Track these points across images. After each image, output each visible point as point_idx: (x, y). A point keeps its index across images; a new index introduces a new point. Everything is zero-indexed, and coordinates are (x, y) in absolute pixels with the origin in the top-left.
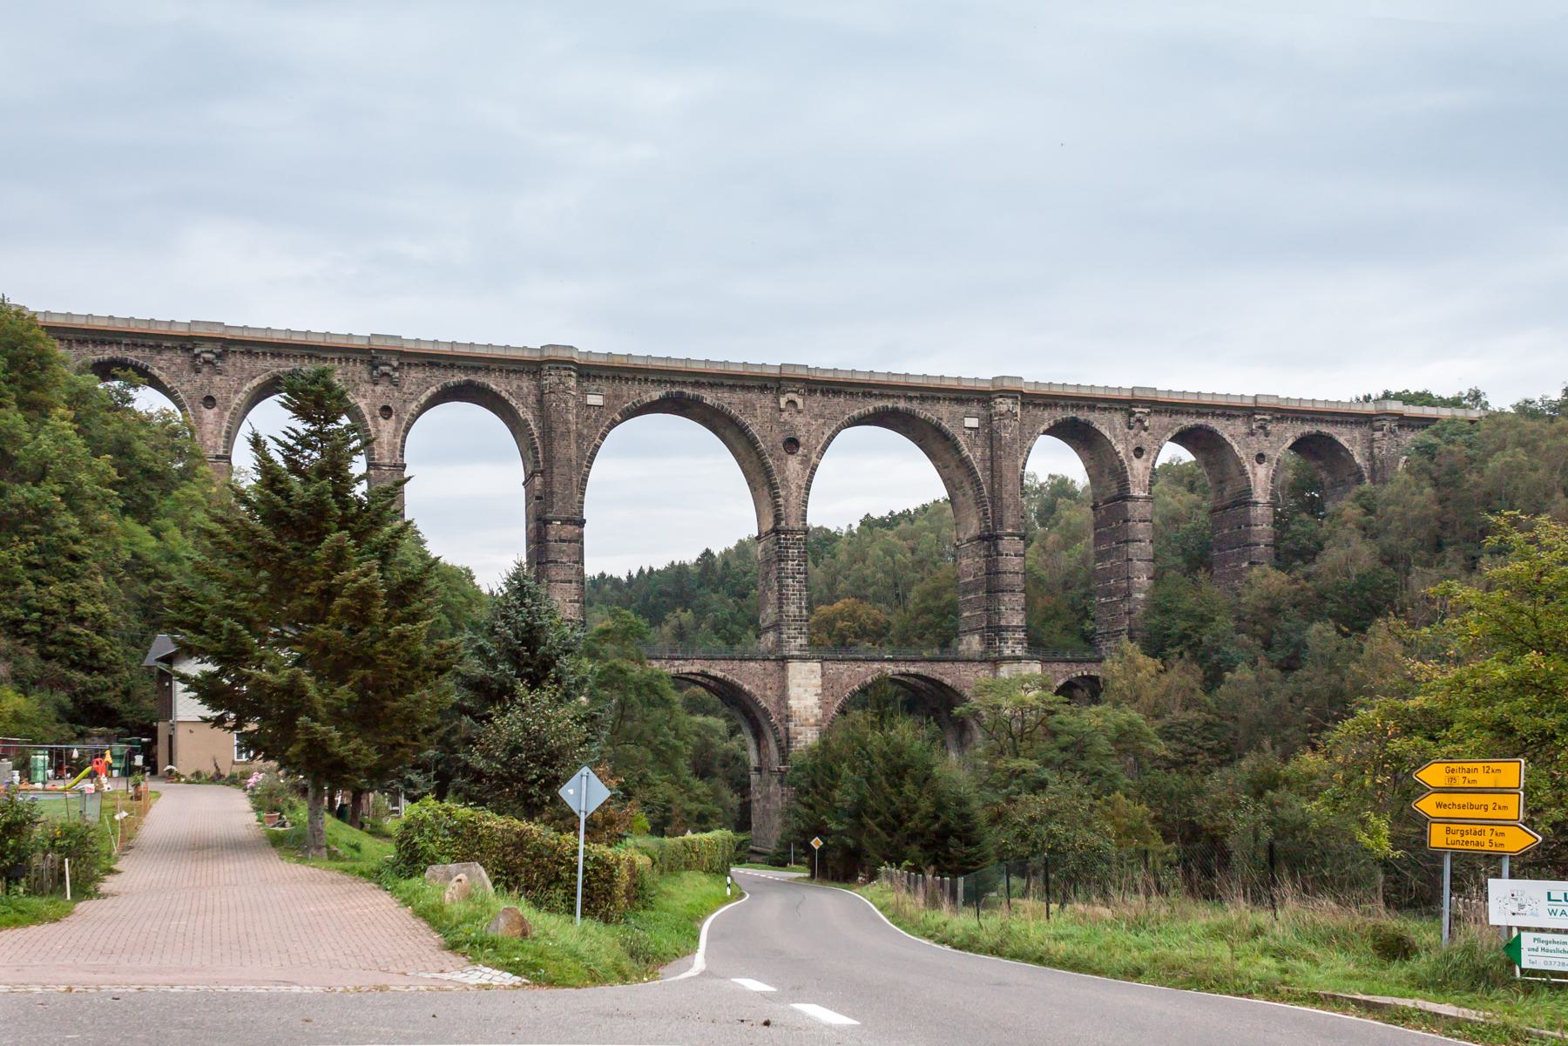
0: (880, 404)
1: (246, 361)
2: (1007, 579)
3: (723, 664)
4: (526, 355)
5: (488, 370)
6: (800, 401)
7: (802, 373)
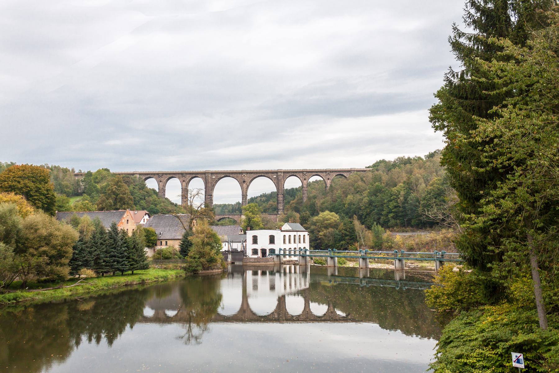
0: (259, 175)
1: (166, 176)
2: (280, 201)
3: (232, 216)
4: (203, 172)
5: (198, 174)
6: (245, 175)
7: (245, 171)
